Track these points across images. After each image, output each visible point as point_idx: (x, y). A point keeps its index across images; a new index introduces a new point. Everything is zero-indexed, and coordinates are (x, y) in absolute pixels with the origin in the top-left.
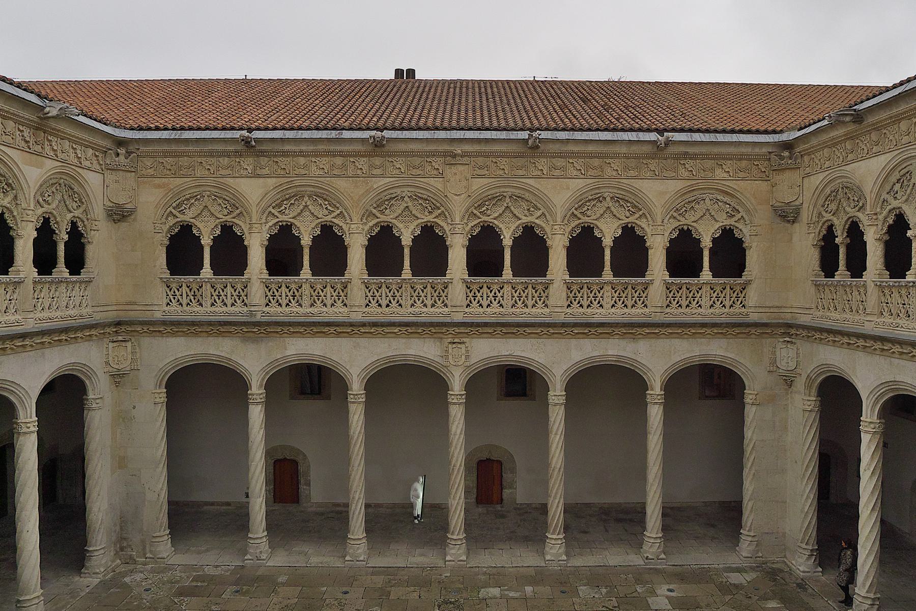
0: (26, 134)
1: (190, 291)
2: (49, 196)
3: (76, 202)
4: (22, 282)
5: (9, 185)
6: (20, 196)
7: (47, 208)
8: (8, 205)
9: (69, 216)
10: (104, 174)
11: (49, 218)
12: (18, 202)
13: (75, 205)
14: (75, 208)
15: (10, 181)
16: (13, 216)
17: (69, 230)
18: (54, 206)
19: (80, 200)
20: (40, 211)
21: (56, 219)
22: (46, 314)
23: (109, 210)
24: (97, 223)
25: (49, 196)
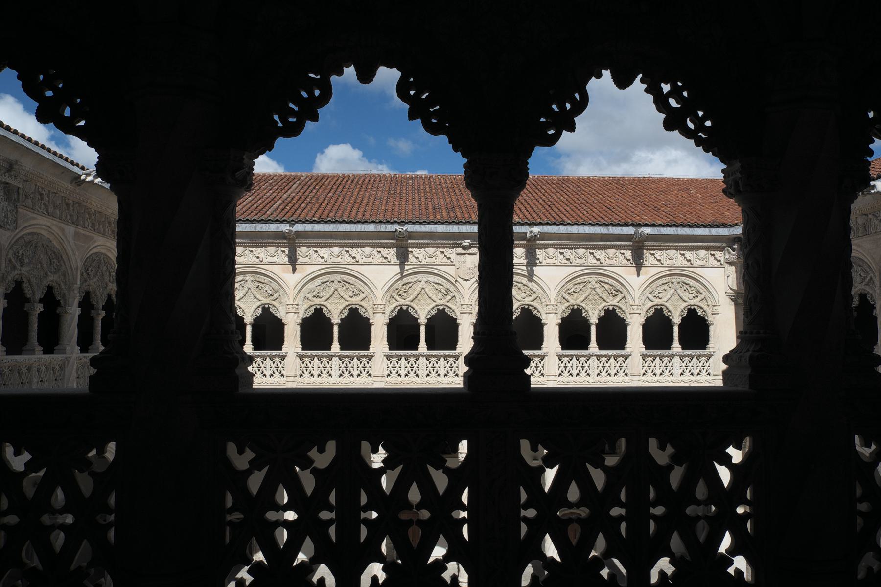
0: (626, 255)
1: (343, 364)
2: (659, 293)
3: (692, 293)
4: (712, 355)
5: (617, 291)
6: (628, 297)
7: (657, 301)
8: (617, 304)
9: (685, 304)
10: (724, 267)
11: (661, 309)
12: (627, 301)
13: (691, 296)
14: (691, 298)
15: (618, 288)
16: (623, 311)
17: (685, 316)
18: (665, 299)
19: (698, 292)
20: (650, 304)
21: (668, 309)
22: (658, 378)
23: (731, 296)
24: (716, 308)
25: (659, 293)
